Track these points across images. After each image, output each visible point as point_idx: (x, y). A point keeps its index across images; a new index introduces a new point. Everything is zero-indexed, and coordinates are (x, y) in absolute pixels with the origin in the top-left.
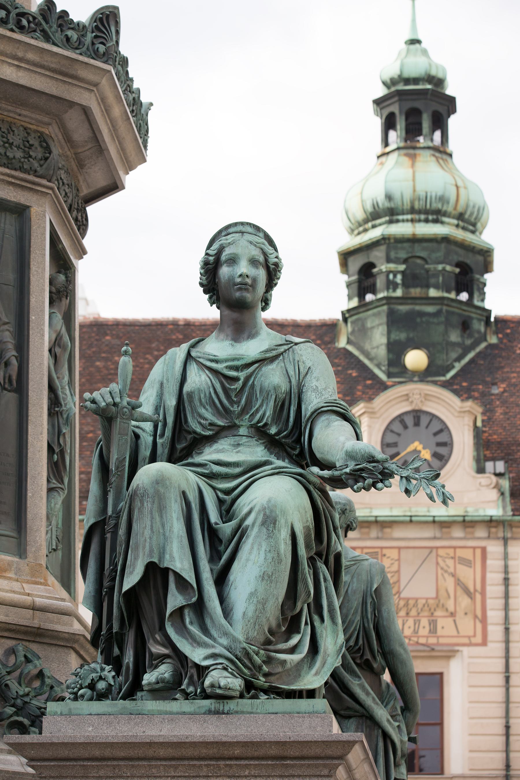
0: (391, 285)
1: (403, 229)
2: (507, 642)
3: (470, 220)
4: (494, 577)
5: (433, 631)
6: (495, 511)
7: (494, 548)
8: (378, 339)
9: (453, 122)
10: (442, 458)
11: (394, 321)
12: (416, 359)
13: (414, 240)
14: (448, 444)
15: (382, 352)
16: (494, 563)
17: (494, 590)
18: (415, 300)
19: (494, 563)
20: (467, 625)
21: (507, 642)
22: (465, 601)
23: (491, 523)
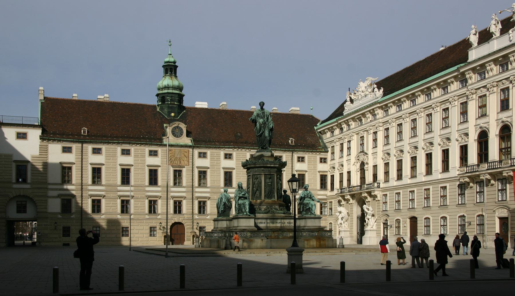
0: (168, 101)
1: (170, 91)
2: (193, 165)
3: (180, 88)
4: (191, 154)
5: (180, 162)
6: (190, 144)
7: (191, 150)
8: (166, 110)
9: (178, 69)
10: (182, 135)
11: (169, 108)
12: (173, 114)
13: (173, 93)
14: (183, 132)
15: (167, 113)
16: (191, 152)
17: (191, 157)
18: (173, 104)
19: (191, 152)
20: (186, 162)
21: (193, 165)
22: (185, 159)
23: (190, 147)
